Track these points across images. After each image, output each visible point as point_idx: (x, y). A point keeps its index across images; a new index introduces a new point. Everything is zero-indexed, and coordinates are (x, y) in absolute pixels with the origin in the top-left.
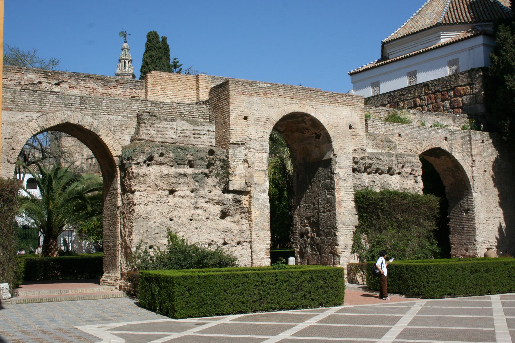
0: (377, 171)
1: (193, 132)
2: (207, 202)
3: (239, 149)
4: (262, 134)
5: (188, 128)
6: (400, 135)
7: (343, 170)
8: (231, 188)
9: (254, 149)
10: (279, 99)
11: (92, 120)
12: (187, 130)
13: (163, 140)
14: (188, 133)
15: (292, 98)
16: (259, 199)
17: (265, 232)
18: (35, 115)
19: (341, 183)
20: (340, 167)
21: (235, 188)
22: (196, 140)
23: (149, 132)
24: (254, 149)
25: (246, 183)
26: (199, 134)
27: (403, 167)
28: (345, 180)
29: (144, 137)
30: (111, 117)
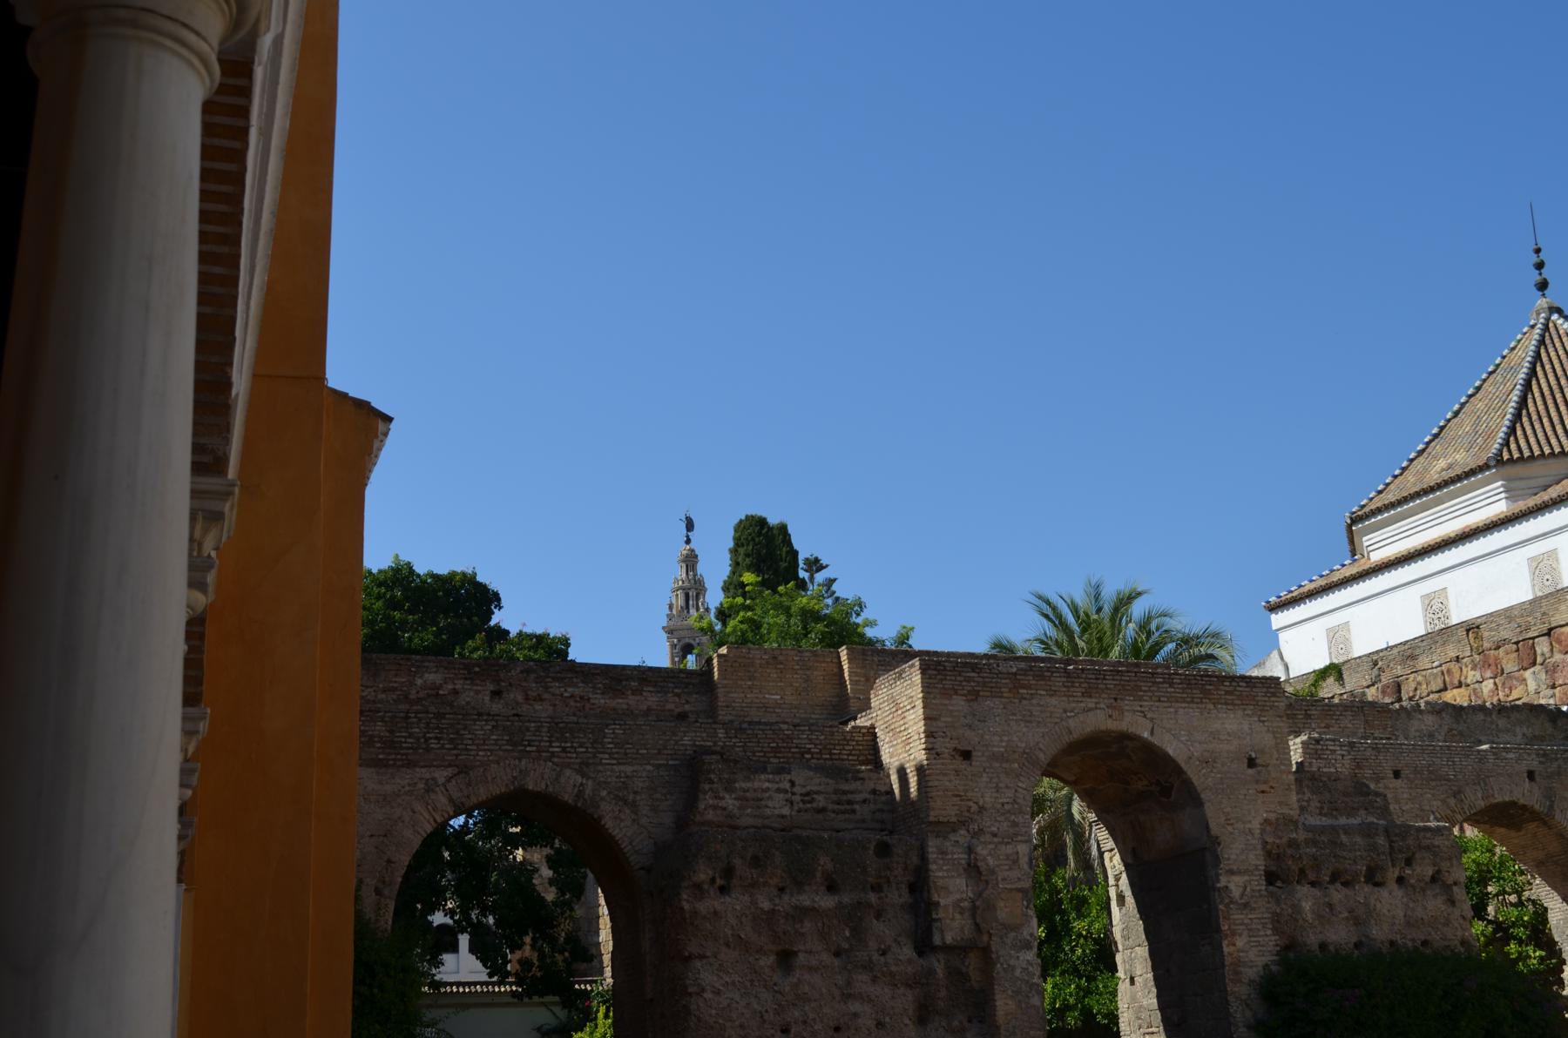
1: (834, 797)
2: (874, 980)
3: (953, 837)
4: (1010, 793)
5: (821, 788)
6: (1397, 774)
7: (1238, 879)
8: (937, 940)
9: (995, 835)
10: (1054, 701)
11: (579, 779)
12: (818, 793)
14: (821, 801)
15: (1087, 694)
16: (1013, 968)
18: (441, 775)
20: (1231, 872)
21: (949, 939)
22: (842, 817)
23: (722, 804)
24: (995, 835)
26: (850, 802)
30: (629, 769)
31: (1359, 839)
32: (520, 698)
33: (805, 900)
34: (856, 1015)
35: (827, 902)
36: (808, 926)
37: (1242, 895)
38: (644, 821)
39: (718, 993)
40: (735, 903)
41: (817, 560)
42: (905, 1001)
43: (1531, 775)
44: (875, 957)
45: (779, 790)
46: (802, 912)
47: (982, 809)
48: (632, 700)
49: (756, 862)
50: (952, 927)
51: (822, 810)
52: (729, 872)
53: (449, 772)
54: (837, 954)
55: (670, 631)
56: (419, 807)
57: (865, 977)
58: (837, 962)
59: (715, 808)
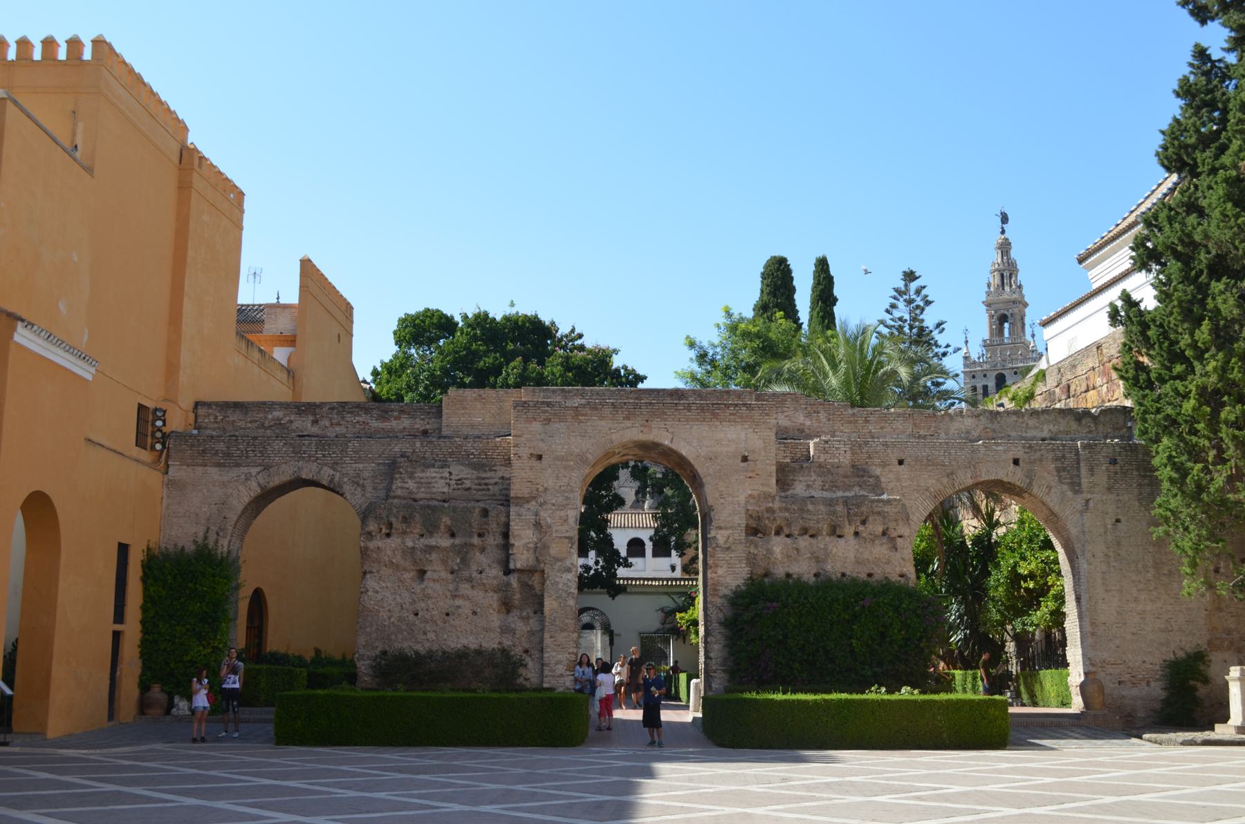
3: (526, 506)
4: (566, 480)
6: (901, 462)
7: (725, 533)
8: (512, 566)
10: (603, 423)
13: (429, 496)
14: (468, 484)
16: (558, 583)
17: (565, 634)
18: (254, 471)
19: (720, 555)
20: (720, 528)
21: (519, 566)
25: (537, 560)
27: (864, 522)
29: (399, 492)
30: (361, 466)
31: (822, 508)
32: (327, 424)
33: (433, 541)
34: (459, 607)
35: (445, 542)
36: (434, 556)
37: (726, 542)
38: (368, 495)
39: (377, 592)
40: (394, 542)
41: (912, 273)
42: (493, 600)
43: (1016, 462)
44: (475, 574)
45: (442, 478)
46: (430, 549)
47: (546, 489)
48: (394, 423)
49: (405, 520)
50: (521, 558)
51: (469, 489)
52: (390, 525)
53: (259, 469)
54: (452, 573)
55: (988, 305)
56: (241, 488)
57: (467, 586)
58: (450, 576)
59: (402, 488)
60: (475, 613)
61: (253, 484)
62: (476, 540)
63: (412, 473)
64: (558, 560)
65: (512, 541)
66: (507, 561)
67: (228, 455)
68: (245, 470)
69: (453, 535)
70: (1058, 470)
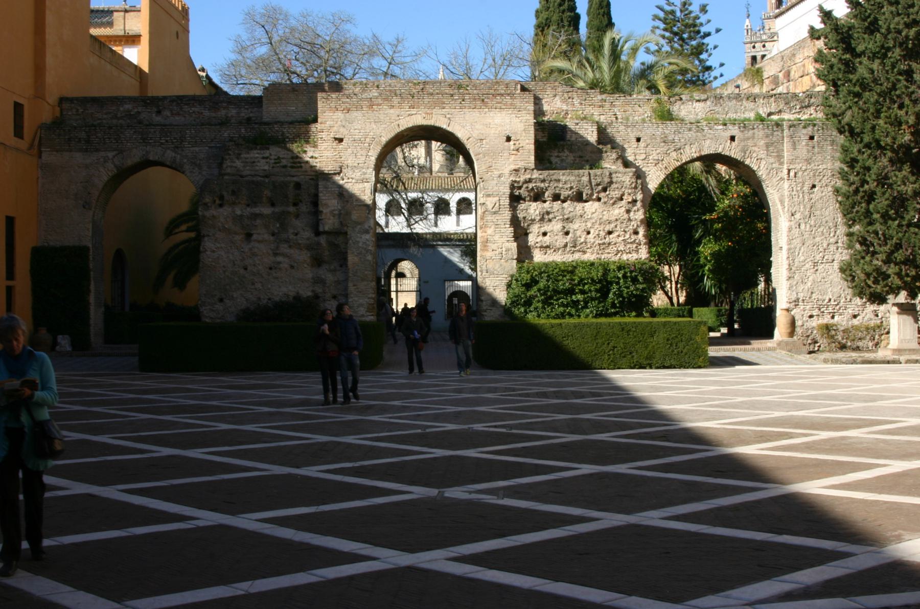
0: (556, 197)
6: (638, 140)
8: (321, 229)
10: (392, 111)
13: (253, 173)
14: (284, 162)
16: (358, 242)
17: (365, 283)
18: (110, 155)
21: (326, 228)
28: (495, 213)
29: (229, 170)
30: (197, 149)
33: (257, 210)
34: (280, 263)
35: (267, 211)
36: (258, 222)
38: (204, 173)
39: (214, 251)
40: (226, 211)
42: (304, 256)
44: (292, 237)
45: (263, 158)
46: (255, 216)
49: (233, 193)
50: (329, 223)
51: (285, 167)
52: (222, 198)
53: (115, 153)
54: (273, 235)
56: (101, 169)
57: (286, 246)
58: (272, 238)
59: (231, 167)
60: (292, 267)
61: (110, 166)
62: (292, 209)
63: (240, 154)
64: (360, 224)
65: (321, 209)
66: (318, 225)
67: (88, 141)
68: (102, 154)
69: (273, 205)
70: (767, 146)
